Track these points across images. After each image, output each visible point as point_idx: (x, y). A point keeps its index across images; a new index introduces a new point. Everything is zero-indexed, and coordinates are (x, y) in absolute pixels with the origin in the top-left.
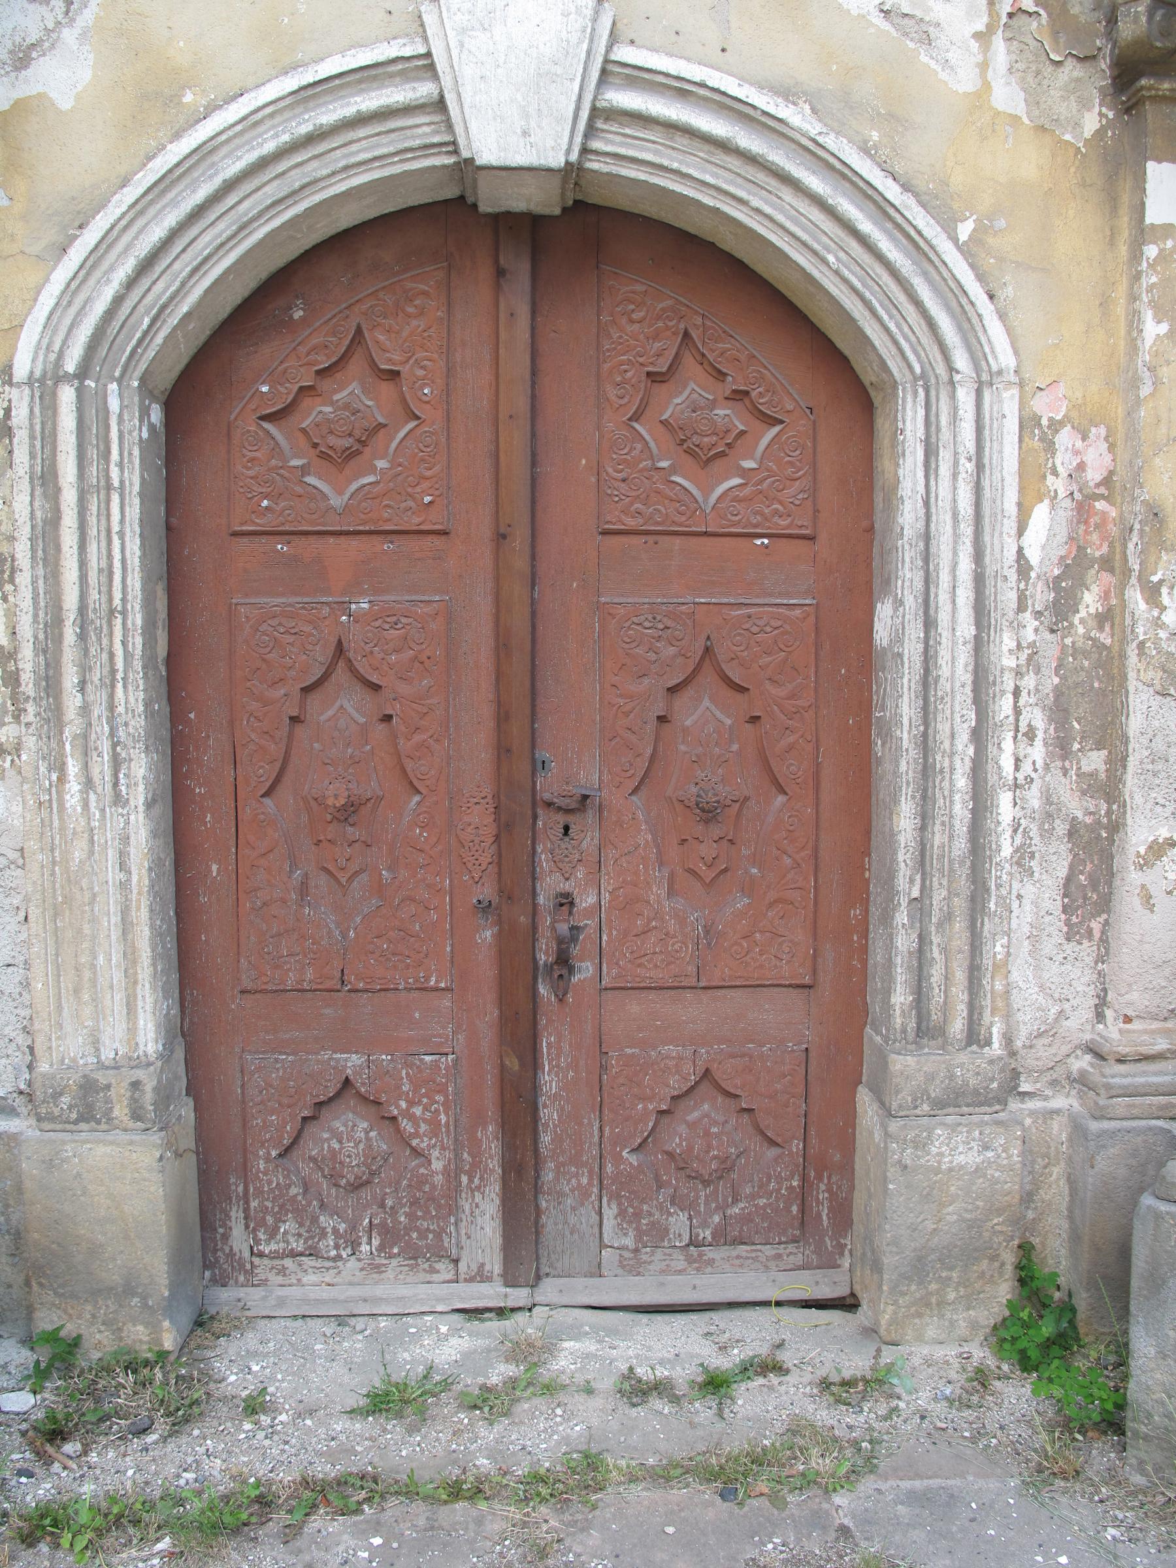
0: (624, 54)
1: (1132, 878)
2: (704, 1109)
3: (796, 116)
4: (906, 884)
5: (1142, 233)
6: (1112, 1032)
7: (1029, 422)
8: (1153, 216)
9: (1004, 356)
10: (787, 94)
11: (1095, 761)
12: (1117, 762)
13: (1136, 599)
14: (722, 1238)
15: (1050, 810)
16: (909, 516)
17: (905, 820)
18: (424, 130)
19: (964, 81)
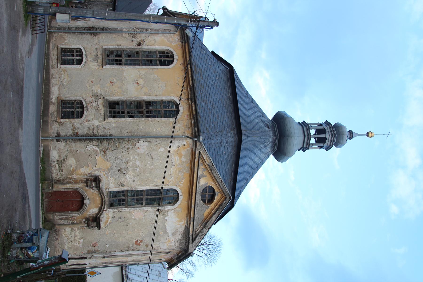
0: (88, 205)
1: (61, 220)
2: (51, 206)
3: (86, 209)
4: (60, 213)
5: (83, 219)
6: (56, 220)
7: (76, 216)
8: (83, 220)
9: (78, 215)
10: (87, 209)
11: (65, 219)
12: (65, 220)
13: (70, 220)
14: (46, 207)
15: (63, 218)
16: (73, 213)
17: (63, 213)
18: (85, 198)
19: (88, 214)
